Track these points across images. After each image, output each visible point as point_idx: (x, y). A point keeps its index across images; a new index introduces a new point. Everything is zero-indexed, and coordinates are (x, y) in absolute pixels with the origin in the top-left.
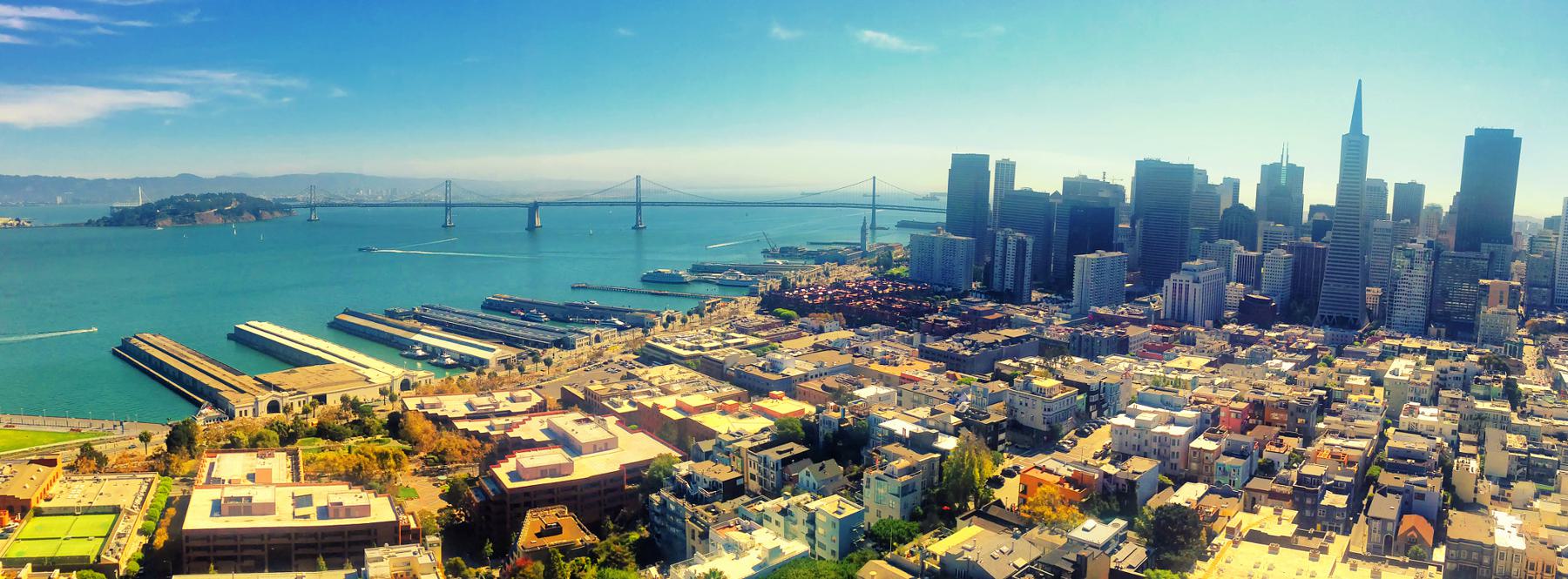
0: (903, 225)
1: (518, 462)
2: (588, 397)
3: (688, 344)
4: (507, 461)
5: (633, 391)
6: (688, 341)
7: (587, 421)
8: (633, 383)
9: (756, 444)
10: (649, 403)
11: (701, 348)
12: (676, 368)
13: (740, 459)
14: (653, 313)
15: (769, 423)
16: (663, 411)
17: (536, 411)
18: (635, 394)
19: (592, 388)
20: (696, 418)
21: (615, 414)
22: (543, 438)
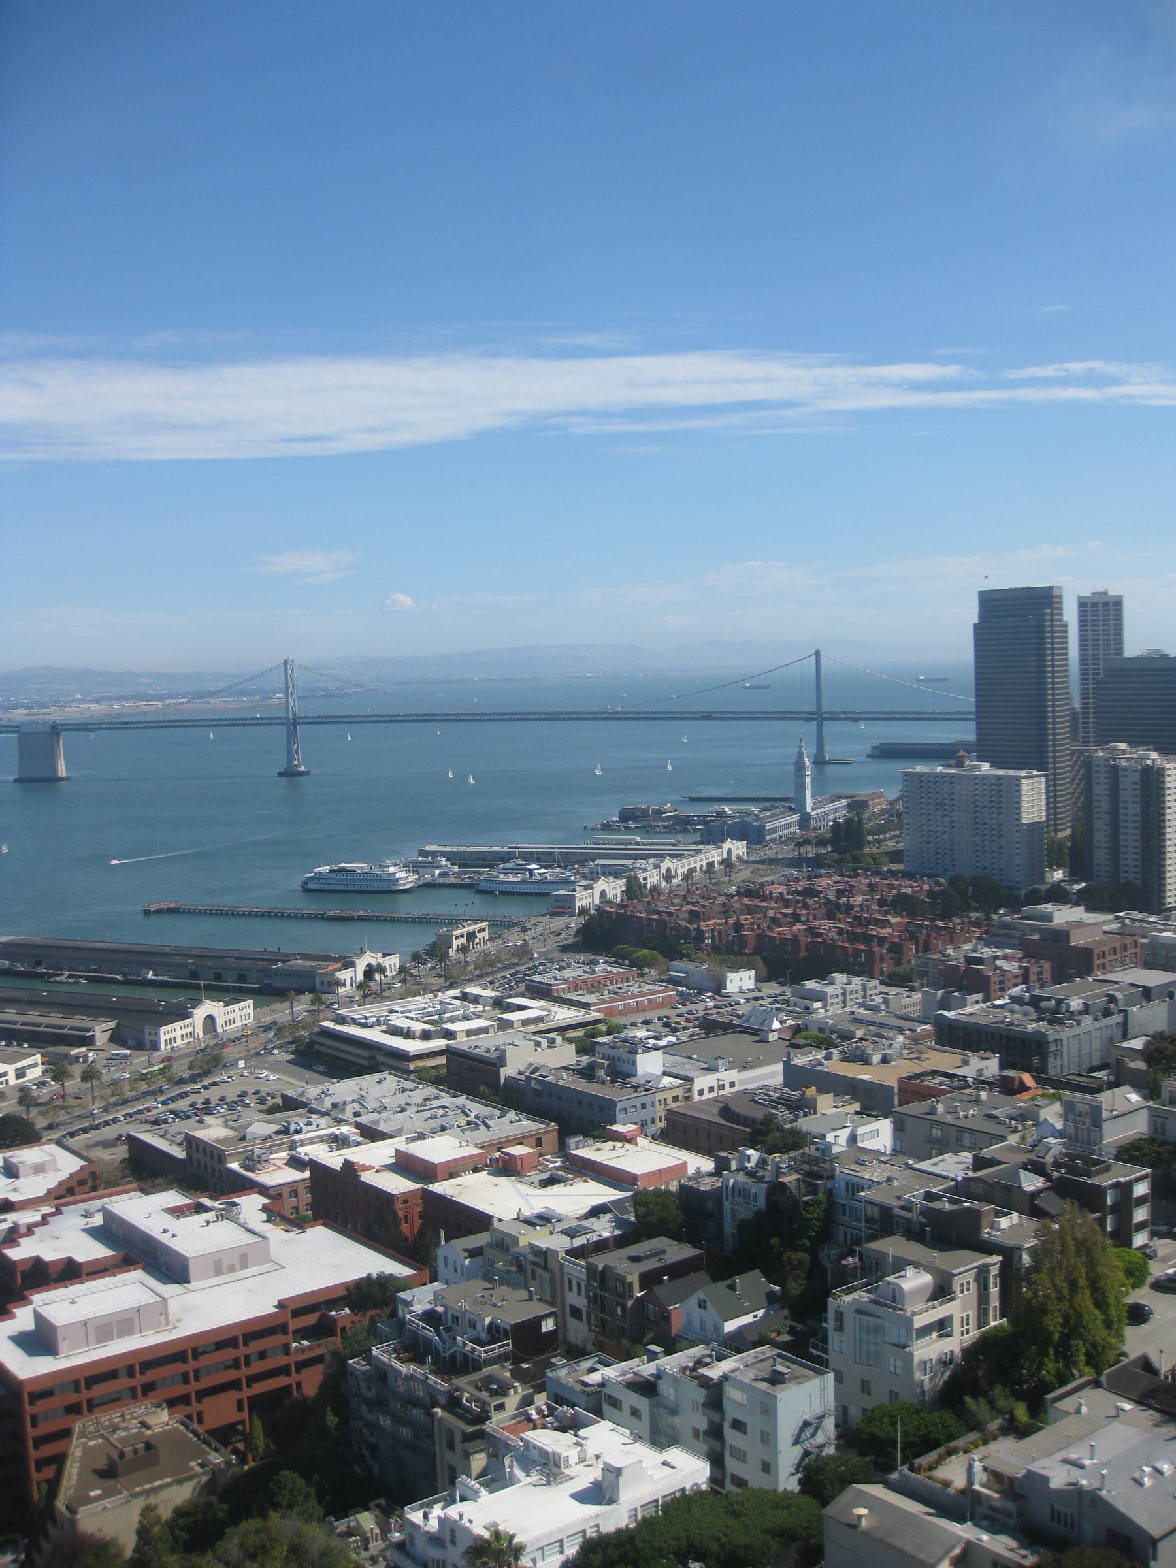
0: (887, 752)
1: (38, 1318)
2: (196, 1156)
3: (418, 1027)
4: (13, 1317)
5: (297, 1137)
6: (417, 1020)
7: (199, 1209)
8: (296, 1119)
9: (579, 1241)
10: (334, 1160)
11: (449, 1035)
12: (391, 1081)
13: (546, 1275)
14: (335, 960)
15: (607, 1194)
16: (367, 1177)
17: (71, 1191)
18: (303, 1143)
19: (201, 1134)
20: (441, 1188)
21: (263, 1190)
22: (92, 1251)
